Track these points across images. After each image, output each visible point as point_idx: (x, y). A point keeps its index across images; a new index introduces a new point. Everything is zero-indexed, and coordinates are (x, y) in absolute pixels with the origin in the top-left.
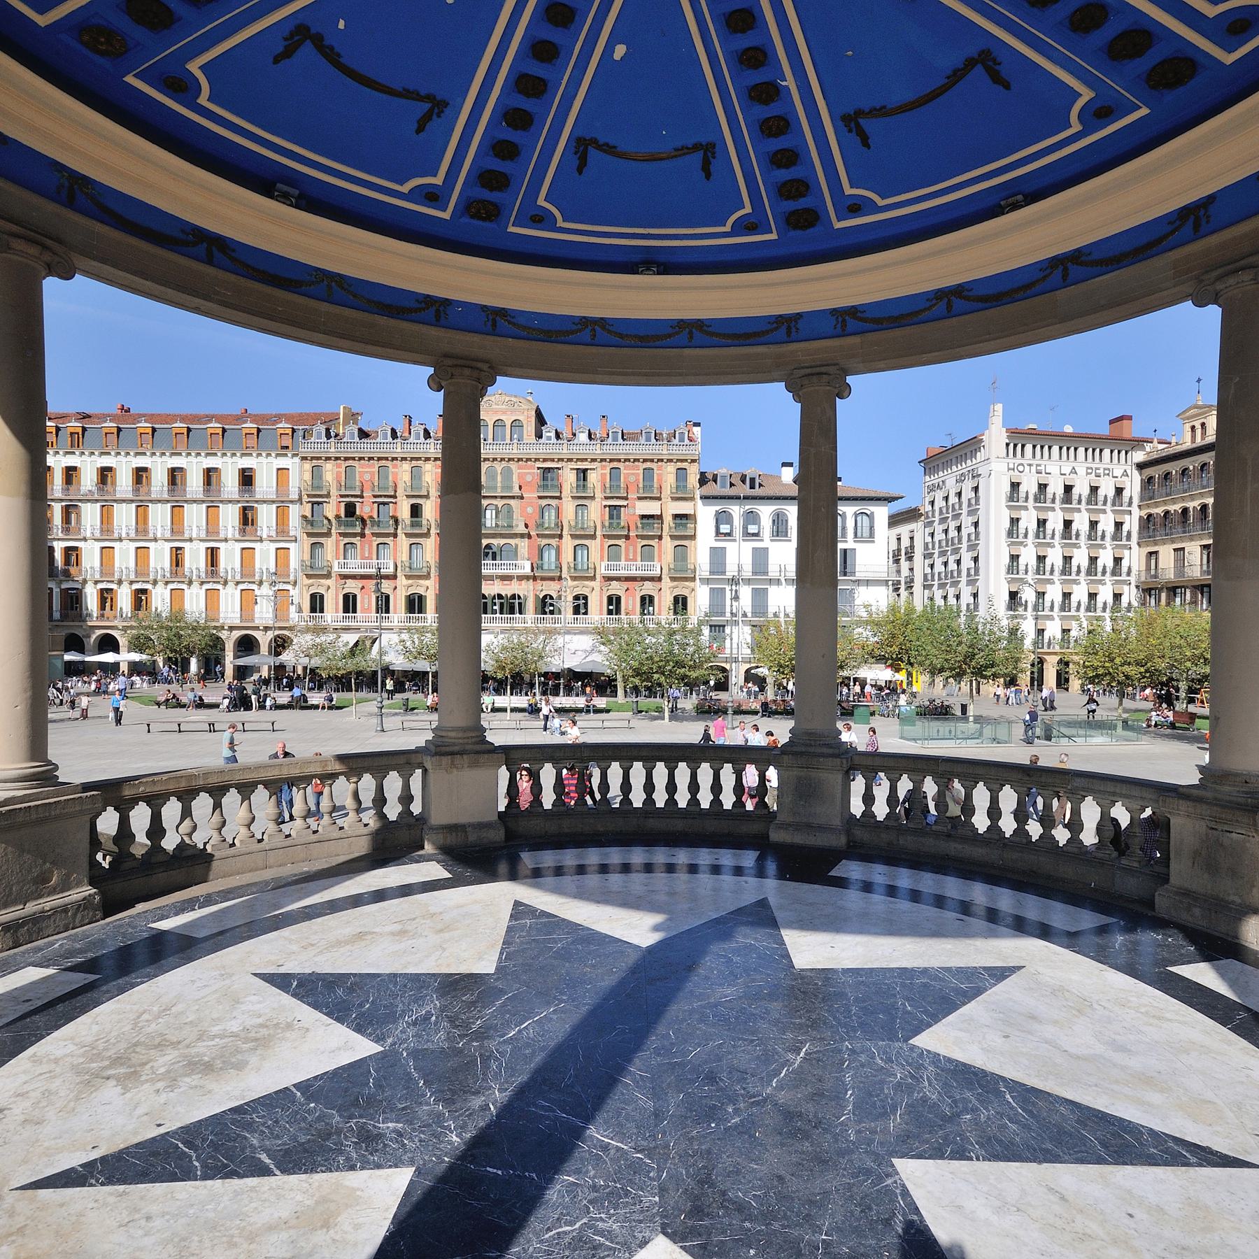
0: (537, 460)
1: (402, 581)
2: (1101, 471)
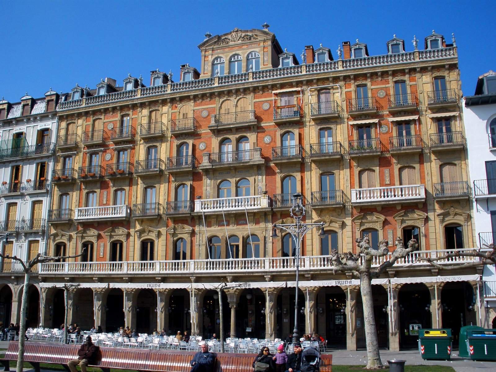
0: (274, 87)
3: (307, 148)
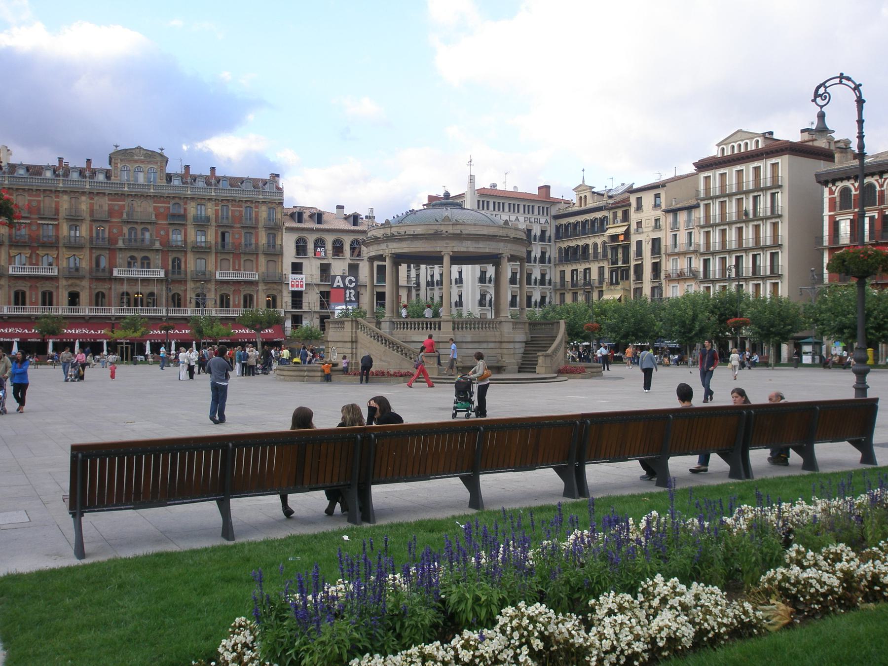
1: (63, 283)
2: (532, 220)
3: (189, 241)
